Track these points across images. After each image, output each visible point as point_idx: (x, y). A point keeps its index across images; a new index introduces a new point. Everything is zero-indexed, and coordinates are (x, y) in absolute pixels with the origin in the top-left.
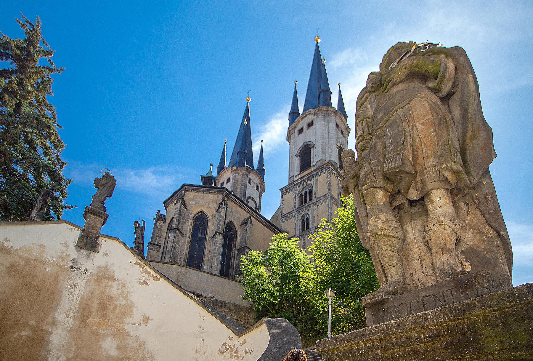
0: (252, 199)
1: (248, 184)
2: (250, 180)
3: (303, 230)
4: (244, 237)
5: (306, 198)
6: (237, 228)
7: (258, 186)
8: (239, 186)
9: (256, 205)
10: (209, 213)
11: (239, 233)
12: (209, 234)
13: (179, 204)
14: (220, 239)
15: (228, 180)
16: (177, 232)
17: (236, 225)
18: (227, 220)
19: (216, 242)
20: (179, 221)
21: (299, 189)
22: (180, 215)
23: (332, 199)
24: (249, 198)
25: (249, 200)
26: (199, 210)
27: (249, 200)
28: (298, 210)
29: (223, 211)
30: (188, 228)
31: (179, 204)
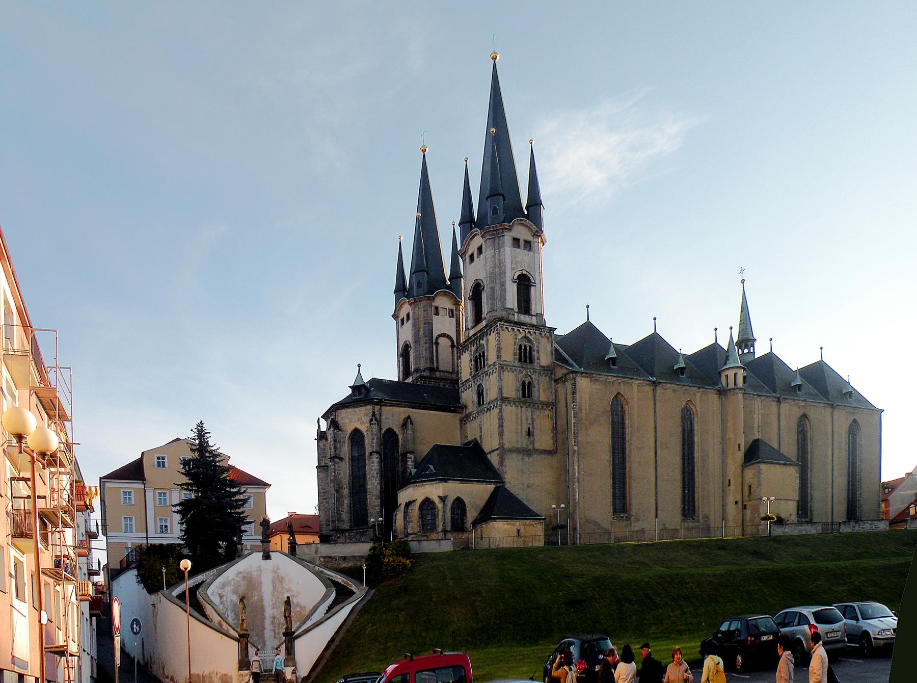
0: (443, 335)
1: (435, 318)
2: (437, 308)
3: (479, 405)
4: (406, 440)
5: (479, 361)
6: (397, 432)
7: (452, 310)
8: (422, 326)
9: (452, 341)
10: (363, 428)
11: (400, 437)
12: (367, 453)
13: (332, 430)
14: (375, 459)
15: (408, 315)
16: (337, 460)
17: (395, 429)
18: (383, 431)
19: (373, 462)
20: (335, 448)
21: (473, 349)
22: (335, 441)
23: (502, 368)
24: (439, 336)
25: (441, 340)
26: (352, 428)
27: (441, 340)
28: (474, 377)
29: (375, 427)
30: (345, 450)
31: (332, 430)
